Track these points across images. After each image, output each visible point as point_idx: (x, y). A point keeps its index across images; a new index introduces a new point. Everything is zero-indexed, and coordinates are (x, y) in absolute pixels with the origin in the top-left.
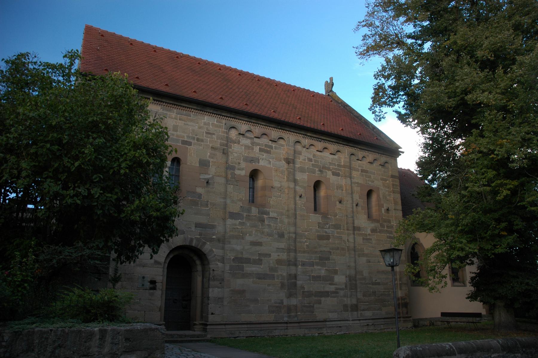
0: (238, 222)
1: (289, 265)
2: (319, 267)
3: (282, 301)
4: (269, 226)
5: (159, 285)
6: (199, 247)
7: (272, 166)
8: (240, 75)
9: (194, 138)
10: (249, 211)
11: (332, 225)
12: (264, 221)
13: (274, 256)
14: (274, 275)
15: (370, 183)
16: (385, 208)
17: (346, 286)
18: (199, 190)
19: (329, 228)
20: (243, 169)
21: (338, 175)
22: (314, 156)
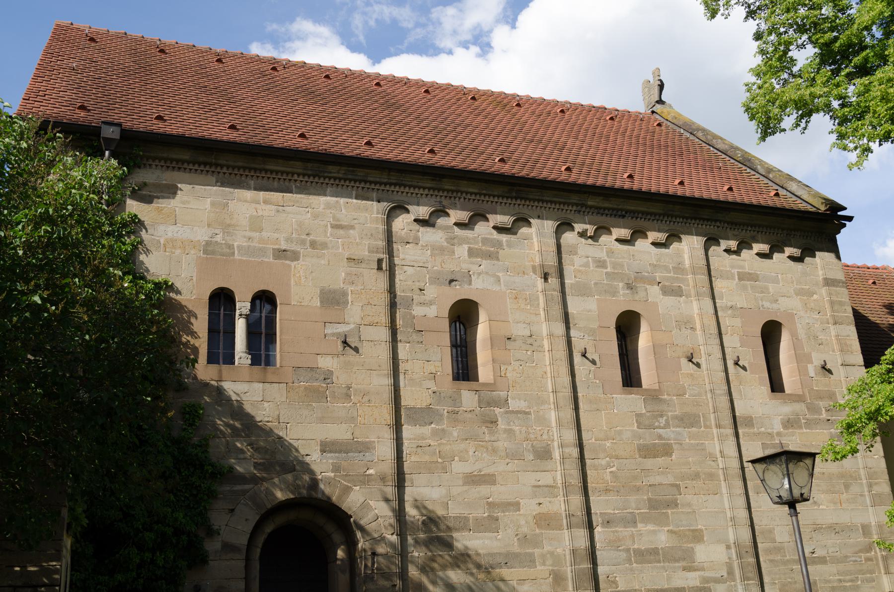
0: (427, 430)
2: (650, 527)
4: (509, 432)
7: (503, 288)
8: (427, 91)
9: (303, 242)
10: (455, 400)
11: (676, 417)
12: (494, 422)
13: (529, 507)
14: (531, 555)
15: (767, 304)
16: (818, 363)
17: (731, 572)
18: (326, 363)
19: (667, 426)
20: (430, 303)
21: (677, 292)
22: (610, 252)
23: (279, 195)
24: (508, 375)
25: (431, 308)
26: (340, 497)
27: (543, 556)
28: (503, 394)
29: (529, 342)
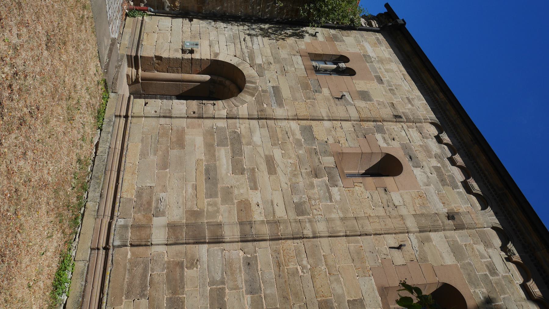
0: (299, 136)
1: (241, 223)
3: (163, 214)
4: (312, 186)
5: (188, 56)
6: (245, 89)
10: (326, 153)
12: (316, 176)
13: (255, 197)
14: (216, 196)
18: (326, 91)
20: (388, 144)
23: (410, 78)
24: (357, 188)
25: (383, 144)
26: (248, 92)
27: (215, 204)
28: (340, 183)
29: (389, 204)
